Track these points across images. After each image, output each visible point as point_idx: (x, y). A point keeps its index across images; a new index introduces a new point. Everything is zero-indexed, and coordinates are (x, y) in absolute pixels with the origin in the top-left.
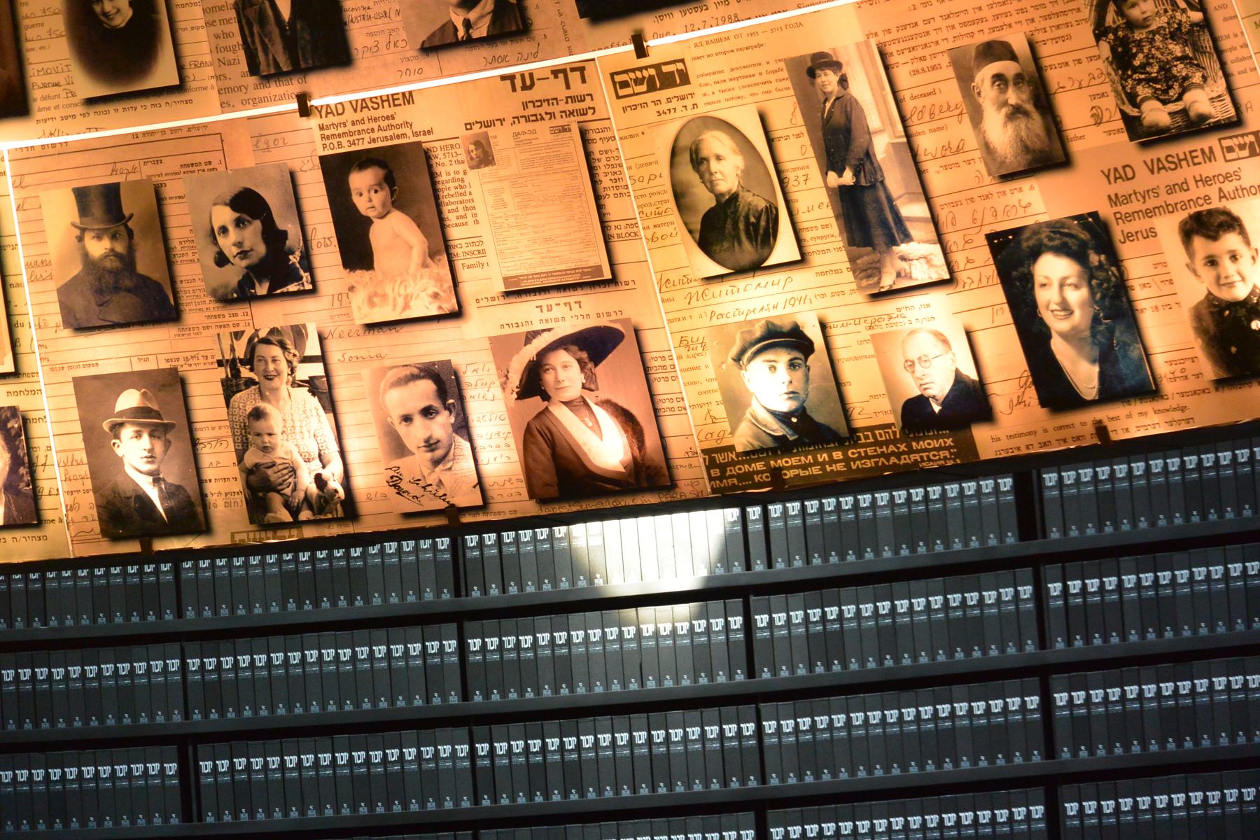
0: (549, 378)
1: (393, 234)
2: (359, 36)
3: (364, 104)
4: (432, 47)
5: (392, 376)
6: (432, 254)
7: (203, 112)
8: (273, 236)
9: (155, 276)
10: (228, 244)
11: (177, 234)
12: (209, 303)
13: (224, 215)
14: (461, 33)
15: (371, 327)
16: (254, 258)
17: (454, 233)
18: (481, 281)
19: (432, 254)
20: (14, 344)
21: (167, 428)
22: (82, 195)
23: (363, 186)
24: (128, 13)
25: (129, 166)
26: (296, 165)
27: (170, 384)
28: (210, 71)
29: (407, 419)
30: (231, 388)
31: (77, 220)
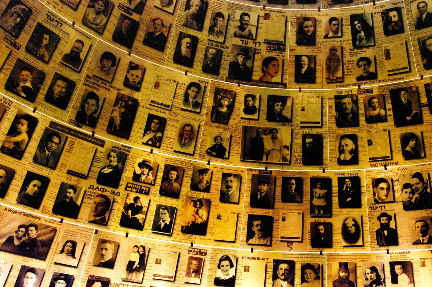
1: (403, 278)
2: (400, 240)
3: (400, 253)
4: (414, 244)
6: (410, 282)
7: (367, 250)
8: (378, 276)
9: (353, 281)
10: (368, 276)
11: (358, 273)
13: (369, 271)
14: (421, 241)
16: (373, 280)
17: (415, 279)
19: (410, 282)
22: (340, 264)
23: (397, 268)
24: (354, 231)
25: (350, 259)
26: (384, 263)
28: (370, 243)
31: (339, 268)
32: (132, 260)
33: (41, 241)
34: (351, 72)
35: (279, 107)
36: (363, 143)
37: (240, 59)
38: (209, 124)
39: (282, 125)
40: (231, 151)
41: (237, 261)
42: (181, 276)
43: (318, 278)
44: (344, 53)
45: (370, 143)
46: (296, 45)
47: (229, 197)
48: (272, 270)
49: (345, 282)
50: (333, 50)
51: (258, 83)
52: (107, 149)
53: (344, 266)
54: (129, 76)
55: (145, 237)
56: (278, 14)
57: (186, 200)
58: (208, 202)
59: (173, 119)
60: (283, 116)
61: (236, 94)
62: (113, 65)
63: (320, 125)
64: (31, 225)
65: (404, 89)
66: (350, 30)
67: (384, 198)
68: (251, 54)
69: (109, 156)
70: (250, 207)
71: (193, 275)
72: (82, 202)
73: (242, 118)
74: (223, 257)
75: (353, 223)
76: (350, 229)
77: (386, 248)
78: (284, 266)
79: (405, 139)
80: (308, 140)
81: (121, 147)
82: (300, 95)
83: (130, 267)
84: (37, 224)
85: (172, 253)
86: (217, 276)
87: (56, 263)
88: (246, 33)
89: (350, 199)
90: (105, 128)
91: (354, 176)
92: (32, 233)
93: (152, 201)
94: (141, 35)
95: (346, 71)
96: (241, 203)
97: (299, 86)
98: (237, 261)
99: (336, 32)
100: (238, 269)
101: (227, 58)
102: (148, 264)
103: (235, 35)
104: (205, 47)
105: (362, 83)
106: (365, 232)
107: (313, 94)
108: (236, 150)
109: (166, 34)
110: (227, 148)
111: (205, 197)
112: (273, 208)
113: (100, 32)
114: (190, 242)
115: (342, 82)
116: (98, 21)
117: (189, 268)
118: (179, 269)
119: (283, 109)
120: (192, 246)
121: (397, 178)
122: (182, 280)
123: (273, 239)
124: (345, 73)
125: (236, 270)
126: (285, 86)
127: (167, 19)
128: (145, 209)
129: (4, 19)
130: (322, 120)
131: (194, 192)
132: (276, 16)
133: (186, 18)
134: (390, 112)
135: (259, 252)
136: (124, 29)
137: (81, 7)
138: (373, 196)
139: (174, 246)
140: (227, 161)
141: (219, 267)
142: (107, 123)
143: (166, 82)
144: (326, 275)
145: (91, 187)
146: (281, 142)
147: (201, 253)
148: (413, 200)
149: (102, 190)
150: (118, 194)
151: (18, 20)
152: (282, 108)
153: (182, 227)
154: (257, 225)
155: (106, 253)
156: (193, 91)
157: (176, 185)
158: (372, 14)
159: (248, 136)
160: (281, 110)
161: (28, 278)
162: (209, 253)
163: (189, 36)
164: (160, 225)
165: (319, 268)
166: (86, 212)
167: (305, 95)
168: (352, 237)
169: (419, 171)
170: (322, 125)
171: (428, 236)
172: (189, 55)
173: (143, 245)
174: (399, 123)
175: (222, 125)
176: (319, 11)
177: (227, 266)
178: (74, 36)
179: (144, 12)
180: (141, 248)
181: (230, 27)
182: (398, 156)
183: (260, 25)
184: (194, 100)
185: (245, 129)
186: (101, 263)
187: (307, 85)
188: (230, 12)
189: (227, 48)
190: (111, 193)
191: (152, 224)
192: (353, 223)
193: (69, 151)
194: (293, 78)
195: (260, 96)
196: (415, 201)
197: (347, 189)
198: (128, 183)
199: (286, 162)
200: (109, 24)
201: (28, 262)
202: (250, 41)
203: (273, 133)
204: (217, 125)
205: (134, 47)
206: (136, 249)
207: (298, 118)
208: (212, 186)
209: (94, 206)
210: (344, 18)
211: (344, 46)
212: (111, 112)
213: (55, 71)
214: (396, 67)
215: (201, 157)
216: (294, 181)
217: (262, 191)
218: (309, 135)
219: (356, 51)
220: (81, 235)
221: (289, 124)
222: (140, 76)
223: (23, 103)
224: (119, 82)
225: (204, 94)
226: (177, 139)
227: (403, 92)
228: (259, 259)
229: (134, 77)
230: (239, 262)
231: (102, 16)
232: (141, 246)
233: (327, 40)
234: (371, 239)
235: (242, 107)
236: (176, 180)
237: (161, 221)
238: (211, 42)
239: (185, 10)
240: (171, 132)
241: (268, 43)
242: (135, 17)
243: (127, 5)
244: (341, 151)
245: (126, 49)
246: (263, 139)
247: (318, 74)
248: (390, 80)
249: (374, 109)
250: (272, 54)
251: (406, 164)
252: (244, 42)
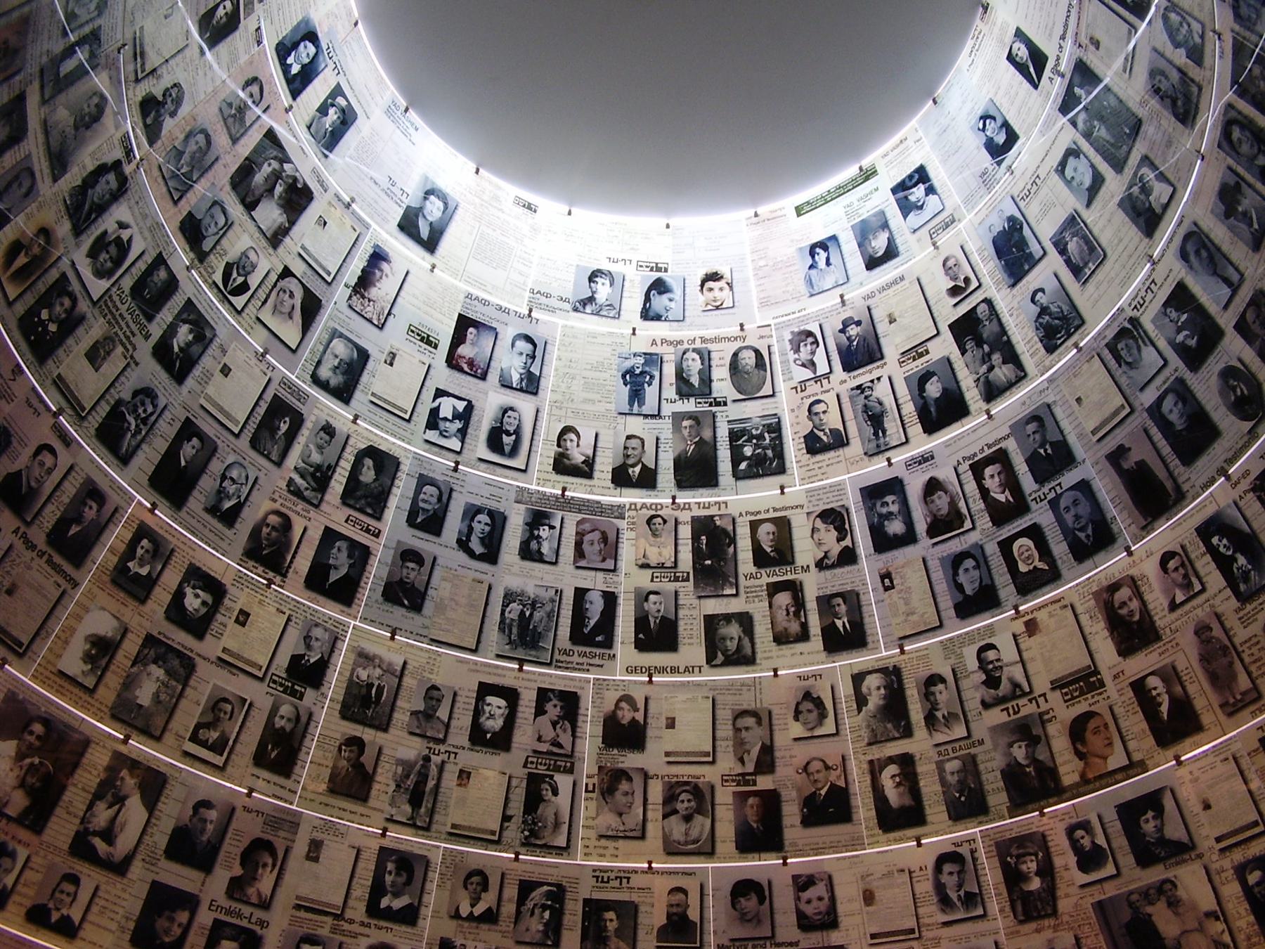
37: (1019, 752)
38: (1018, 932)
39: (1178, 863)
44: (1228, 625)
46: (1120, 659)
50: (1202, 631)
54: (803, 907)
56: (1051, 608)
60: (1171, 842)
61: (1044, 836)
62: (761, 902)
66: (1213, 565)
68: (1037, 731)
73: (1083, 886)
80: (1254, 877)
82: (1183, 771)
88: (1005, 687)
94: (791, 812)
95: (1253, 668)
97: (1170, 753)
99: (1189, 585)
101: (989, 765)
103: (986, 705)
104: (934, 766)
107: (1211, 759)
109: (842, 783)
113: (709, 852)
115: (1260, 697)
116: (694, 833)
119: (1163, 825)
124: (1254, 675)
126: (1142, 766)
127: (829, 750)
129: (522, 927)
132: (1051, 615)
133: (868, 726)
136: (752, 816)
137: (650, 826)
146: (1194, 907)
151: (547, 914)
152: (1158, 822)
156: (951, 873)
158: (1235, 503)
160: (1160, 829)
163: (891, 760)
172: (908, 801)
175: (1046, 922)
176: (1130, 554)
178: (661, 886)
179: (778, 763)
181: (966, 695)
183: (1025, 655)
184: (962, 893)
185: (1100, 906)
188: (952, 661)
189: (981, 742)
194: (1150, 741)
195: (1100, 817)
200: (718, 825)
202: (1021, 702)
203: (1165, 890)
204: (1033, 925)
205: (787, 843)
210: (1186, 542)
211: (1219, 610)
218: (1249, 862)
219: (1249, 607)
222: (826, 896)
225: (976, 870)
229: (815, 903)
231: (698, 819)
233: (1179, 612)
235: (1072, 860)
238: (942, 748)
239: (859, 710)
241: (1061, 687)
242: (764, 783)
243: (739, 769)
245: (774, 855)
246: (1150, 916)
247: (1199, 704)
250: (1081, 707)
252: (1011, 711)
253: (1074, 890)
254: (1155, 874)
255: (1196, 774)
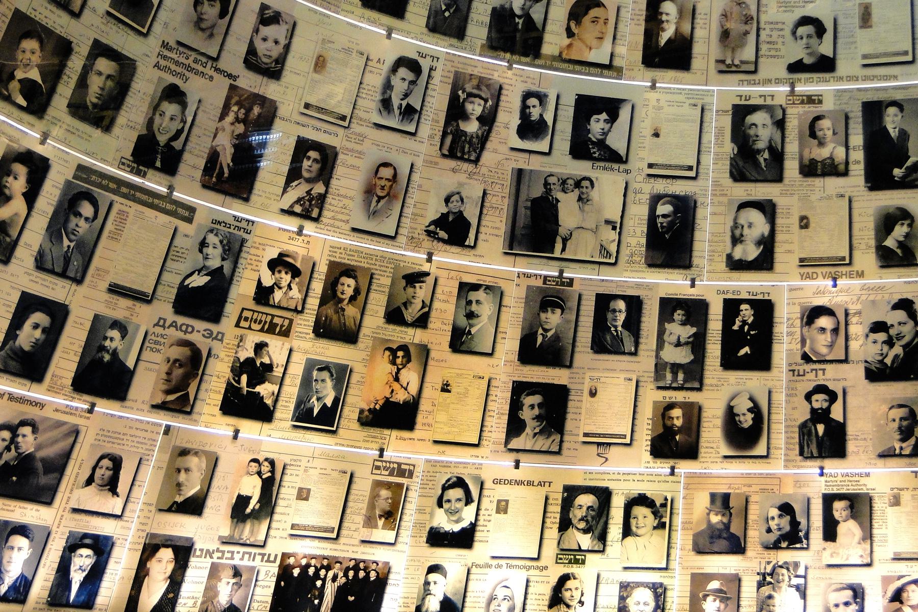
0: (905, 595)
1: (848, 529)
2: (851, 446)
4: (882, 456)
5: (834, 587)
6: (864, 539)
7: (776, 467)
8: (795, 524)
9: (737, 534)
10: (773, 525)
11: (752, 517)
12: (759, 548)
13: (775, 512)
14: (897, 452)
15: (830, 566)
16: (784, 532)
17: (875, 531)
18: (883, 552)
19: (864, 539)
20: (668, 555)
21: (728, 599)
22: (713, 496)
23: (839, 507)
24: (750, 422)
25: (736, 486)
26: (811, 495)
27: (736, 580)
28: (783, 452)
29: (837, 606)
30: (760, 585)
31: (709, 506)
32: (244, 493)
33: (43, 460)
34: (777, 50)
35: (601, 125)
36: (787, 221)
38: (436, 163)
39: (605, 169)
40: (482, 229)
41: (482, 489)
42: (353, 527)
43: (662, 526)
45: (804, 223)
47: (472, 339)
48: (559, 509)
49: (720, 537)
51: (555, 64)
52: (200, 225)
53: (723, 501)
55: (277, 438)
57: (374, 348)
58: (425, 351)
59: (352, 150)
60: (608, 148)
63: (692, 174)
64: (23, 423)
65: (894, 103)
67: (824, 351)
69: (203, 244)
70: (518, 363)
71: (381, 522)
72: (138, 360)
73: (513, 149)
74: (448, 480)
75: (751, 405)
76: (742, 418)
77: (818, 463)
78: (586, 500)
79: (887, 221)
80: (664, 209)
81: (231, 221)
82: (653, 96)
83: (240, 510)
84: (36, 419)
85: (335, 474)
86: (435, 525)
87: (75, 511)
89: (746, 350)
90: (198, 174)
91: (760, 297)
92: (26, 442)
93: (296, 352)
95: (764, 48)
96: (497, 354)
98: (482, 489)
100: (483, 507)
102: (281, 502)
105: (800, 80)
106: (773, 426)
107: (681, 98)
108: (494, 228)
110: (474, 222)
111: (416, 341)
112: (570, 366)
114: (377, 446)
117: (372, 506)
118: (348, 511)
119: (609, 131)
120: (381, 455)
121: (859, 307)
122: (355, 534)
123: (566, 438)
125: (478, 509)
128: (278, 372)
130: (698, 162)
131: (391, 327)
134: (858, 156)
135: (531, 467)
138: (799, 346)
139: (341, 458)
140: (473, 252)
141: (440, 505)
142: (202, 163)
143: (341, 56)
144: (678, 520)
145: (161, 323)
146: (599, 211)
147: (401, 473)
148: (888, 361)
149: (184, 328)
150: (220, 337)
152: (607, 126)
153: (362, 411)
154: (532, 407)
155: (187, 480)
156: (404, 79)
157: (351, 311)
159: (523, 197)
161: (12, 548)
162: (418, 472)
164: (312, 409)
165: (664, 505)
166: (147, 384)
167: (664, 97)
168: (744, 435)
169: (910, 297)
170: (697, 173)
171: (912, 441)
173: (270, 456)
174: (878, 179)
175: (465, 166)
177: (459, 500)
180: (266, 464)
182: (866, 258)
184: (404, 103)
185: (520, 174)
186: (175, 502)
187: (671, 74)
190: (203, 335)
191: (292, 406)
192: (751, 405)
193: (114, 237)
194: (639, 55)
195: (558, 97)
196: (893, 362)
197: (742, 327)
198: (243, 309)
199: (608, 259)
201: (12, 511)
204: (452, 163)
206: (254, 467)
207: (642, 154)
208: (433, 314)
209: (165, 368)
212: (211, 133)
213: (93, 35)
214: (881, 49)
215: (413, 243)
216: (621, 305)
217: (546, 327)
220: (133, 439)
221: (623, 167)
222: (283, 42)
223: (20, 121)
224: (233, 60)
225: (426, 88)
226: (359, 197)
227: (892, 110)
228: (530, 483)
229: (270, 44)
230: (485, 492)
232: (266, 460)
234: (787, 443)
235: (516, 121)
236: (353, 299)
237: (314, 399)
240: (348, 181)
244: (736, 240)
246: (558, 201)
247: (698, 49)
248: (866, 78)
249: (821, 144)
251: (881, 278)
253: (505, 149)
254: (582, 168)
255: (662, 103)
